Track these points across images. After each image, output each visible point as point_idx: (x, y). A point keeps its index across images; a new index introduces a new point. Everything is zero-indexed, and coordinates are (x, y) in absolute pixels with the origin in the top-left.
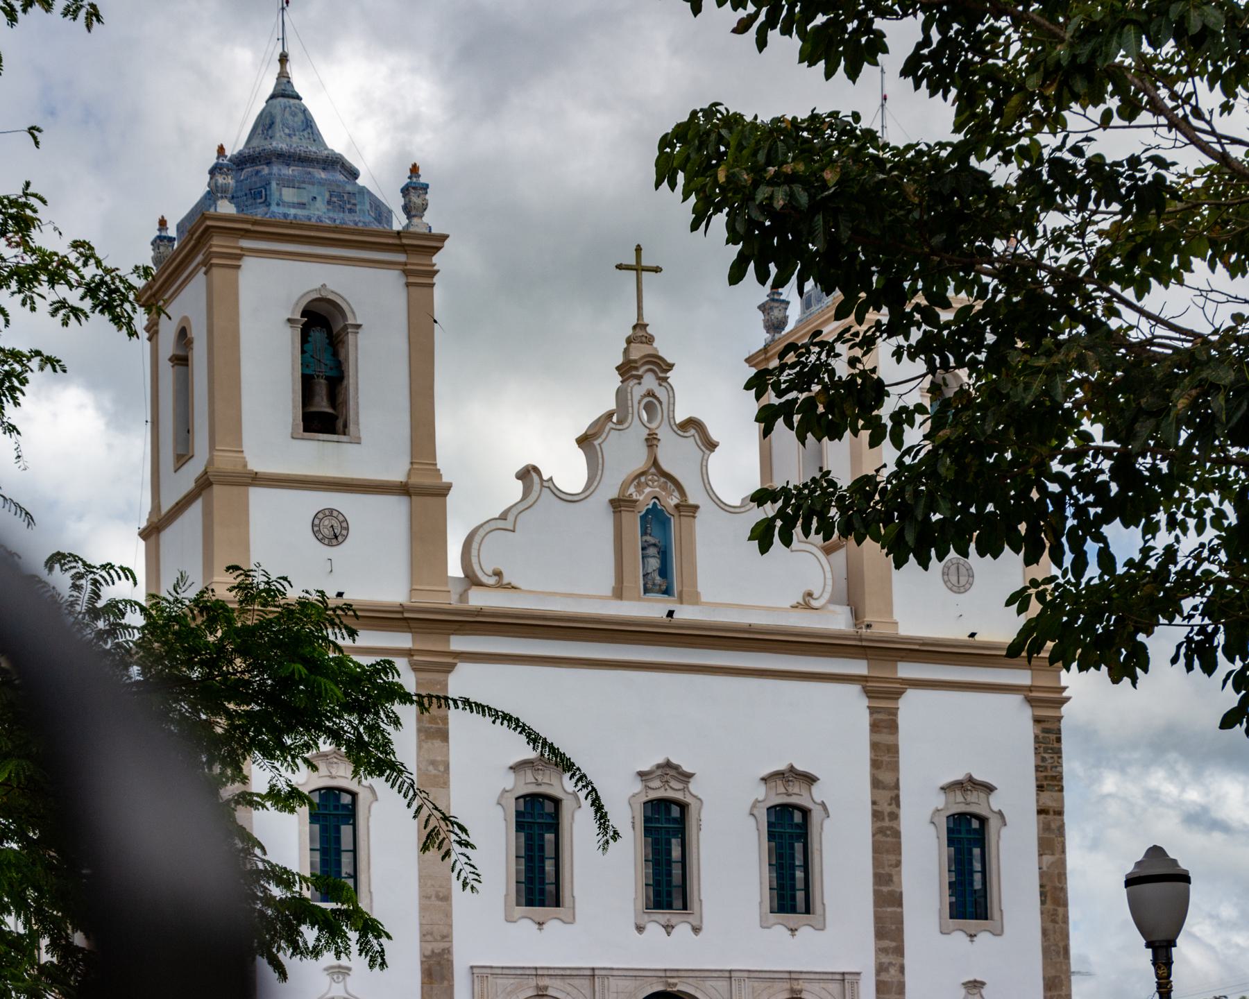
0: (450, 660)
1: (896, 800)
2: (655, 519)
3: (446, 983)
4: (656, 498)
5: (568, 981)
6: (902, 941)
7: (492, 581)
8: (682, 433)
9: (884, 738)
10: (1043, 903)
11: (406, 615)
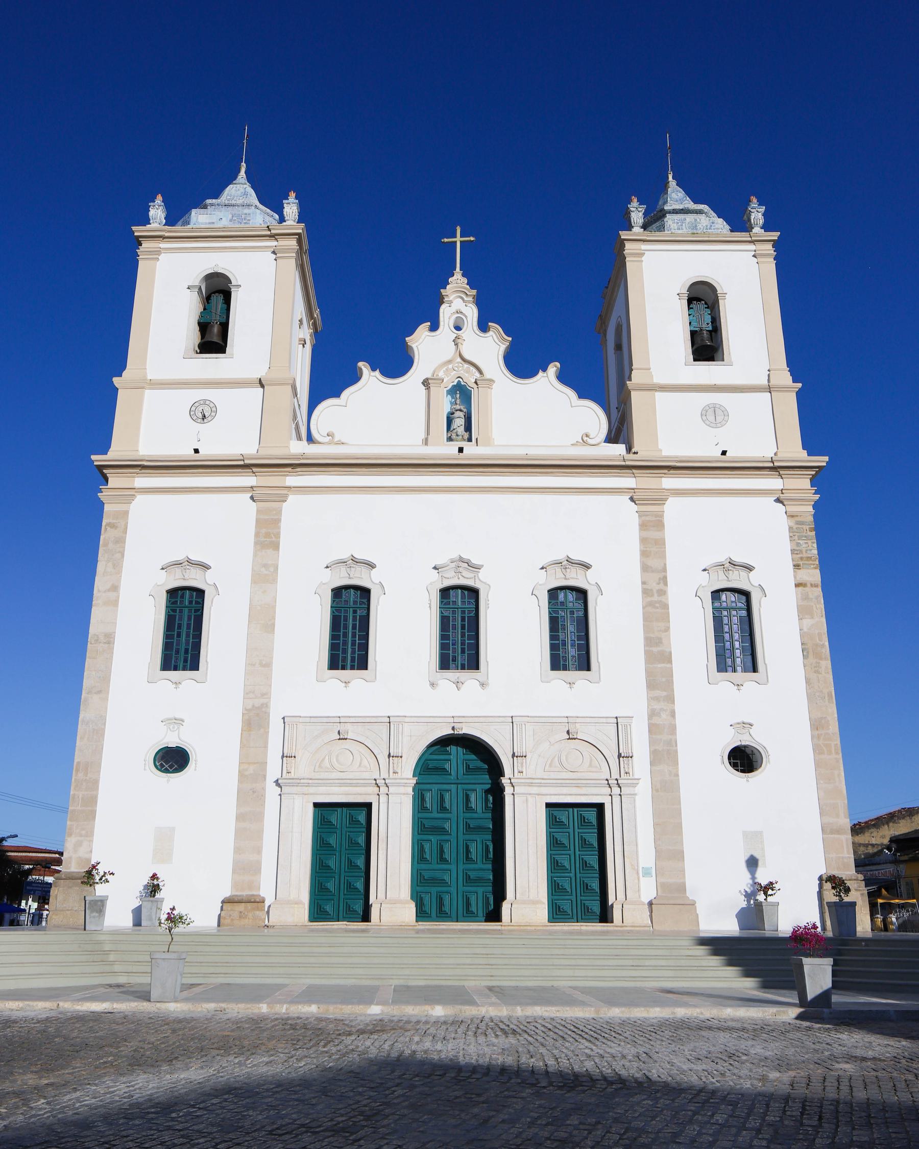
0: (285, 492)
1: (664, 580)
2: (461, 392)
3: (262, 730)
4: (459, 377)
6: (673, 690)
7: (328, 439)
8: (483, 335)
9: (653, 534)
10: (805, 657)
11: (247, 462)
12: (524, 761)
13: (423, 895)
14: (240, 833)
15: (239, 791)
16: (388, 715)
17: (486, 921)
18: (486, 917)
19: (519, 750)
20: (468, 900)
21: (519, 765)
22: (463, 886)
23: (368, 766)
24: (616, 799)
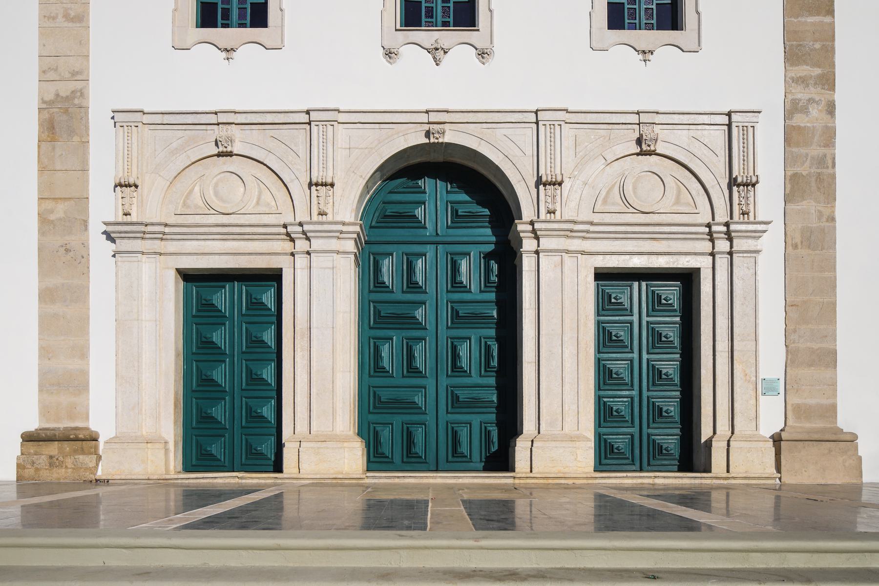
3: (76, 139)
5: (272, 133)
6: (833, 65)
12: (558, 192)
13: (379, 428)
14: (46, 323)
15: (40, 249)
16: (305, 109)
17: (486, 469)
18: (485, 462)
19: (549, 172)
20: (455, 434)
21: (549, 200)
22: (447, 412)
23: (273, 203)
24: (722, 262)
